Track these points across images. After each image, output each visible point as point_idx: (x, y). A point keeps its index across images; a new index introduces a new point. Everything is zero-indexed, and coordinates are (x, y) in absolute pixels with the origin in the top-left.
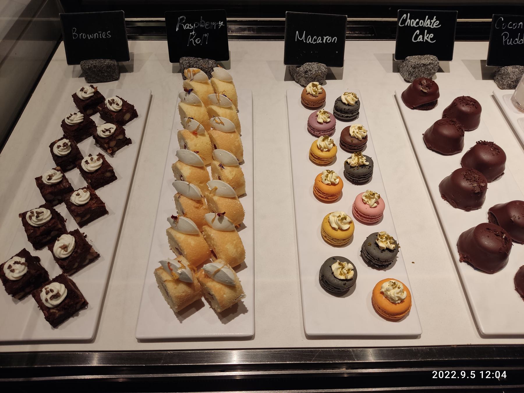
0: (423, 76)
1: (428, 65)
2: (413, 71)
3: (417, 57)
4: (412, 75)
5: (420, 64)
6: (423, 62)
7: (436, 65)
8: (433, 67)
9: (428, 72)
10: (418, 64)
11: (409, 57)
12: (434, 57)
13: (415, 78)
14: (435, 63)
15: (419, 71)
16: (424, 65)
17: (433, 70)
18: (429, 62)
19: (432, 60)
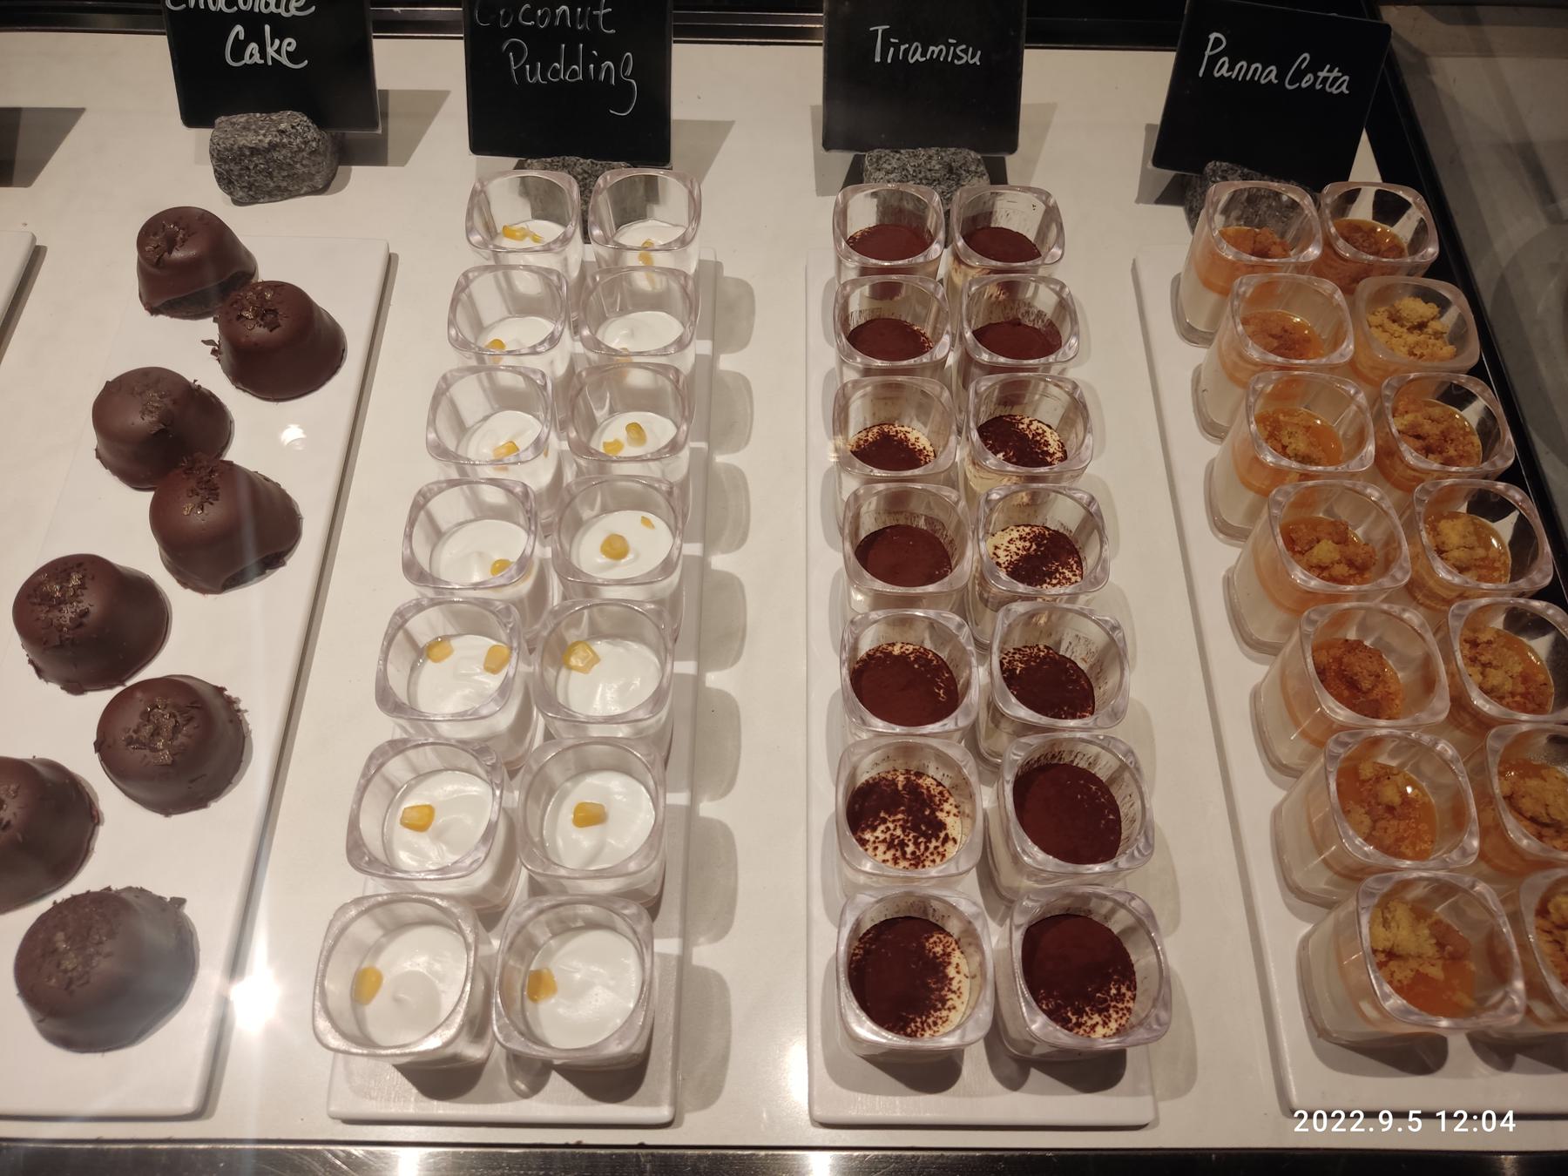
0: (272, 185)
1: (268, 150)
2: (227, 172)
3: (243, 120)
4: (230, 182)
5: (236, 146)
6: (250, 140)
7: (300, 150)
8: (289, 155)
9: (285, 173)
10: (226, 149)
11: (223, 118)
12: (300, 119)
13: (250, 189)
14: (290, 143)
15: (248, 168)
16: (254, 151)
17: (298, 166)
18: (267, 140)
19: (282, 132)
